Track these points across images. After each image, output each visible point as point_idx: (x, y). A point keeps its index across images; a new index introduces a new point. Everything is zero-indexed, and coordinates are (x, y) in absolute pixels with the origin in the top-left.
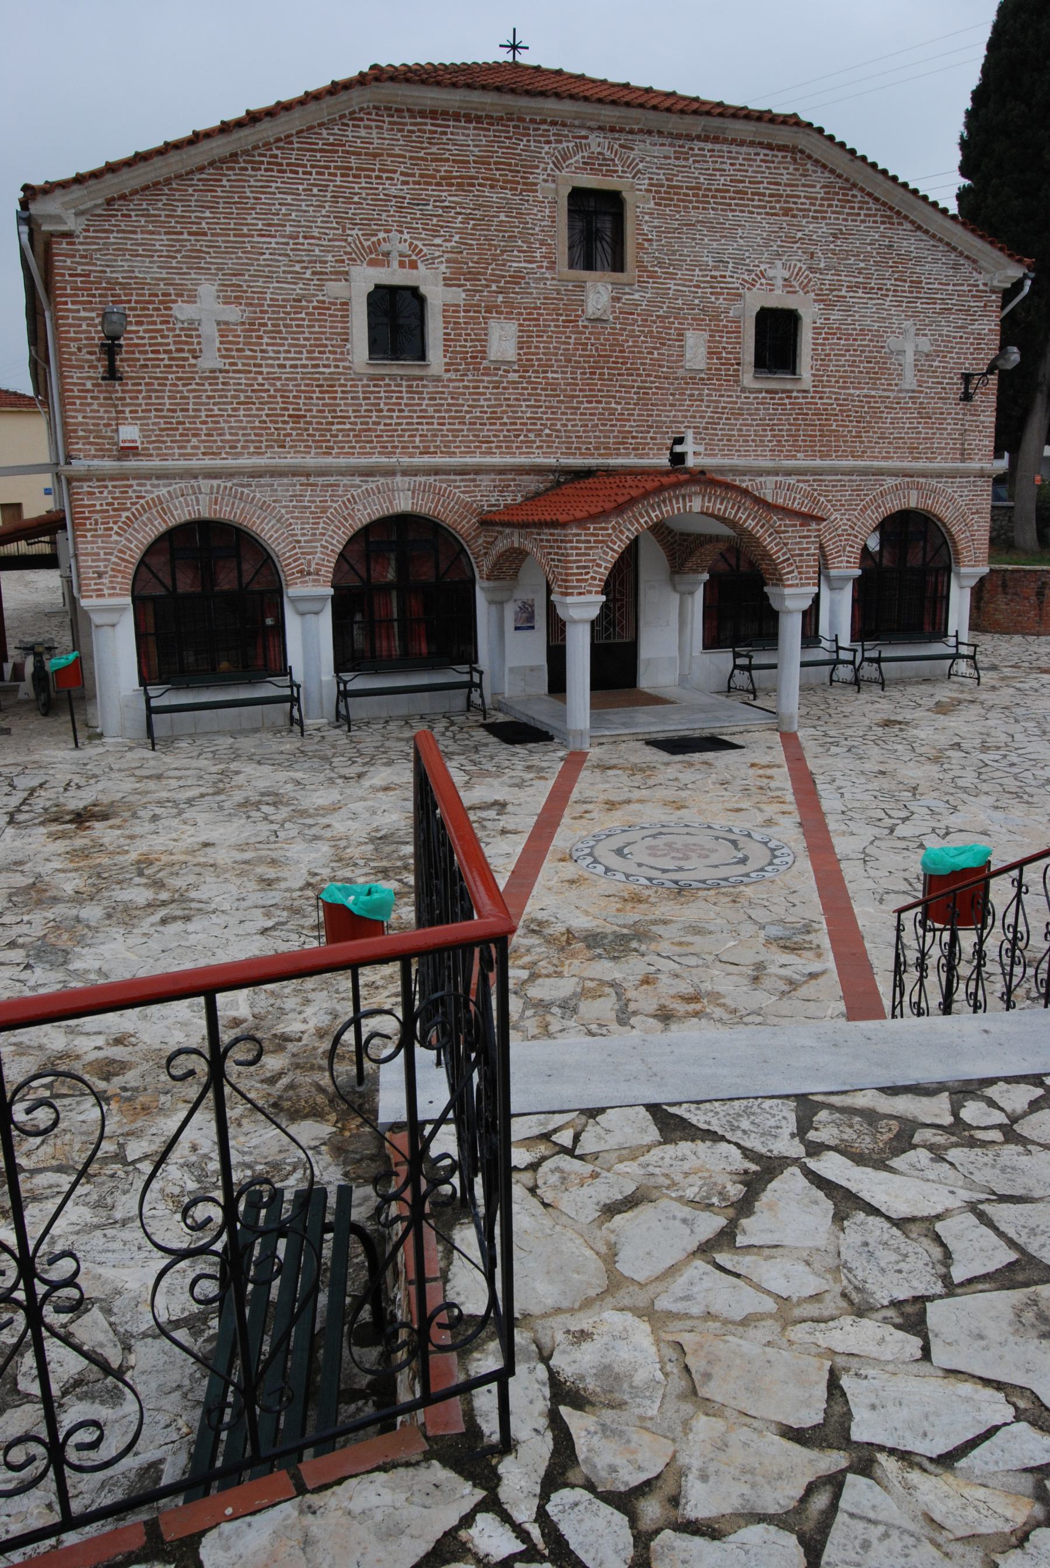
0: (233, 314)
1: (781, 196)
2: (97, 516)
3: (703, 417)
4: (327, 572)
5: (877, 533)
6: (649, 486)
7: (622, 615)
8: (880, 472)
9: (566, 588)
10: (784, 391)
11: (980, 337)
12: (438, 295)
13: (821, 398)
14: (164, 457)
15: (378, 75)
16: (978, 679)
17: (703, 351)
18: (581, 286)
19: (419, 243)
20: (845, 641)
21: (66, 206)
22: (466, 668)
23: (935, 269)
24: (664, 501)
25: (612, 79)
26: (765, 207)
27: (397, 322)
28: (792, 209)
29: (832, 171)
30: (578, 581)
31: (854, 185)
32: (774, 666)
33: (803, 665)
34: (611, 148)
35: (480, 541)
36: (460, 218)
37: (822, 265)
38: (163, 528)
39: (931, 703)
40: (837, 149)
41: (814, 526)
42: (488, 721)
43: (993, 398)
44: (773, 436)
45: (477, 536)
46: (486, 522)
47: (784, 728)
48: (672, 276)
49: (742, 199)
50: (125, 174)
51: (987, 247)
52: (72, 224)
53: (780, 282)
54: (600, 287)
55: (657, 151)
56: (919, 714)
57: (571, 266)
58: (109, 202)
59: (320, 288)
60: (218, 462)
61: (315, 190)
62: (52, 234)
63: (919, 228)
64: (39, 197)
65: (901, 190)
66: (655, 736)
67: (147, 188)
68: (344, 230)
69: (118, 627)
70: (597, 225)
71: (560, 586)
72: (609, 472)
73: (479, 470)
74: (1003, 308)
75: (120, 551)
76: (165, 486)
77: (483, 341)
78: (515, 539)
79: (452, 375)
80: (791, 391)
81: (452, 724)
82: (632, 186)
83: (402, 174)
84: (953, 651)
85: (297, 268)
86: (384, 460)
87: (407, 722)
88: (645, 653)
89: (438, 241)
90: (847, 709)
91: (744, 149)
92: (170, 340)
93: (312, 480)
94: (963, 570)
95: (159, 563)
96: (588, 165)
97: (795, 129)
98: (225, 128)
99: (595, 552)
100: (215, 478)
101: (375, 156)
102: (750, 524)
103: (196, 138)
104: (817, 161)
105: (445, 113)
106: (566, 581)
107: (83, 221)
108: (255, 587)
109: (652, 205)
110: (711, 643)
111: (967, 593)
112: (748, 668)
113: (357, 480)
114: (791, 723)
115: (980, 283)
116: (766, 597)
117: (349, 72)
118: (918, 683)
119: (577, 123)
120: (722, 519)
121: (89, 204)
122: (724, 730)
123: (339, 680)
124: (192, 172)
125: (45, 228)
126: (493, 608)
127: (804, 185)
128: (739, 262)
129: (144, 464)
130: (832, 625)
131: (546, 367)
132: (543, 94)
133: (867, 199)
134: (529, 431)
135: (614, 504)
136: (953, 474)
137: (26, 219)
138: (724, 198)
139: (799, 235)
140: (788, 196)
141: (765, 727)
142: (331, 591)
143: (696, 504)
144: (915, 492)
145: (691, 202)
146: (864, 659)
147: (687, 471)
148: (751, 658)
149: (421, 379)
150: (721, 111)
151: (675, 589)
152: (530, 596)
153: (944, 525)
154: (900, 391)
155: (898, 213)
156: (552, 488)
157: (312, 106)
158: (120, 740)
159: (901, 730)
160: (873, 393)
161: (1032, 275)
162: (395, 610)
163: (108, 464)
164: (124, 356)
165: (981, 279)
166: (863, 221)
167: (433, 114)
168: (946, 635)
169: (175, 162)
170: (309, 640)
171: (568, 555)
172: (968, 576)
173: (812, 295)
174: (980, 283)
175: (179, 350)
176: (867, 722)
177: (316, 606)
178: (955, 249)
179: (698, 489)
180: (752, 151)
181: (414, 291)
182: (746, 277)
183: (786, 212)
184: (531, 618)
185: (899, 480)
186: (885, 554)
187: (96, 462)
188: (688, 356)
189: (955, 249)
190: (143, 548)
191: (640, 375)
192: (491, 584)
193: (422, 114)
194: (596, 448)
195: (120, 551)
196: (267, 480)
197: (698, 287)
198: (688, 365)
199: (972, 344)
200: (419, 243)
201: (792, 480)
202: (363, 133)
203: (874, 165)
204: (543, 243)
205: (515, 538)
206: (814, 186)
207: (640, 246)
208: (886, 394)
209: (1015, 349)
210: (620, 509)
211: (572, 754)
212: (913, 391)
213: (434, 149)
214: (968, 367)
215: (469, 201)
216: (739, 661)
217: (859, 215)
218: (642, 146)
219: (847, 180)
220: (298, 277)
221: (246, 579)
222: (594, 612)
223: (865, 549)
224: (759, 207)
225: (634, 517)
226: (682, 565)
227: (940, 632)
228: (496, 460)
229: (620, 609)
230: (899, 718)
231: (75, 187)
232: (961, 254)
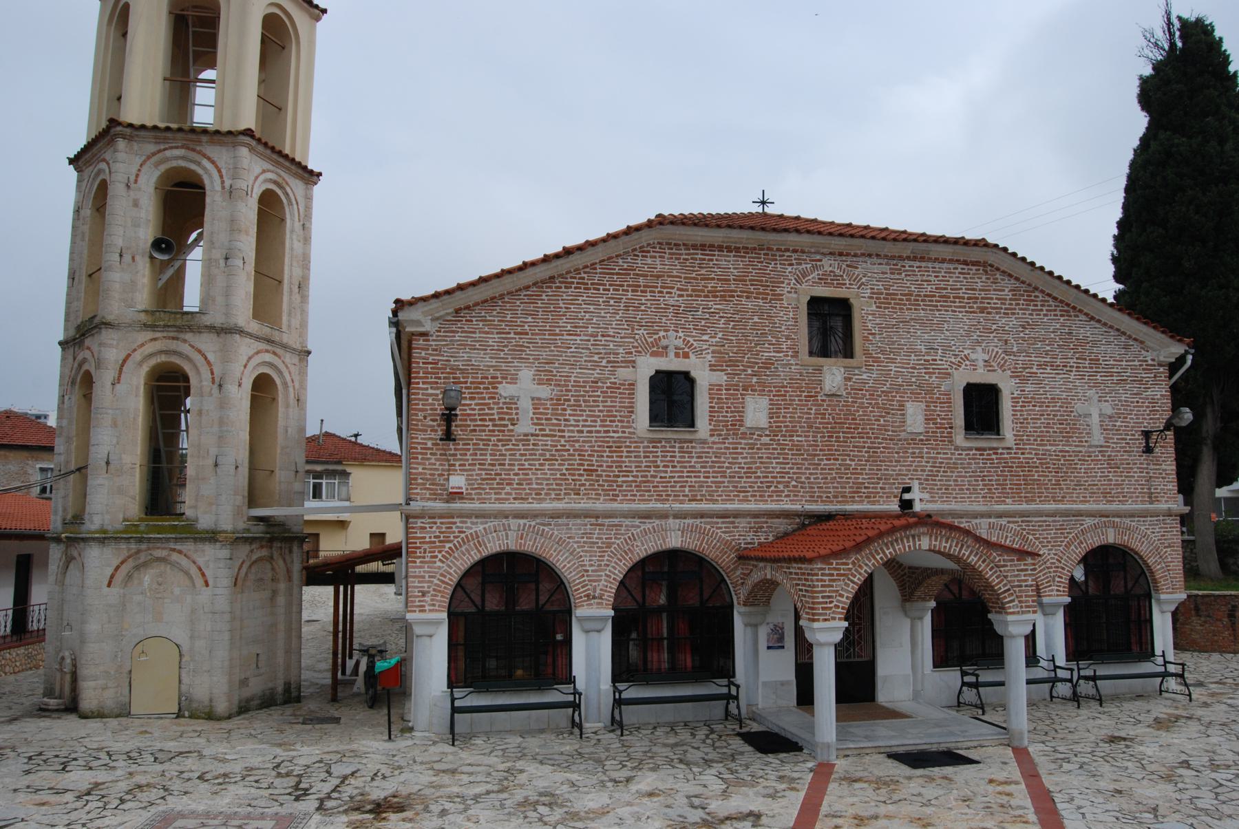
0: (544, 392)
2: (426, 546)
4: (609, 597)
6: (883, 527)
7: (860, 637)
8: (1079, 514)
9: (813, 614)
10: (990, 449)
11: (1153, 401)
12: (704, 378)
14: (483, 501)
15: (661, 221)
16: (1190, 695)
17: (920, 418)
18: (819, 369)
19: (691, 340)
20: (1061, 660)
21: (425, 314)
22: (724, 681)
23: (1108, 349)
24: (896, 541)
25: (837, 221)
27: (672, 398)
29: (1017, 279)
30: (823, 608)
31: (1036, 289)
32: (1002, 684)
33: (1029, 682)
34: (840, 267)
35: (738, 573)
36: (723, 321)
37: (1015, 349)
38: (477, 557)
39: (1150, 719)
40: (1020, 263)
41: (1029, 561)
42: (744, 730)
43: (1172, 450)
45: (735, 569)
46: (743, 557)
47: (1016, 744)
48: (893, 361)
50: (471, 291)
51: (1152, 331)
52: (428, 326)
53: (981, 364)
54: (835, 371)
55: (876, 268)
56: (1140, 730)
57: (811, 354)
58: (457, 311)
59: (613, 373)
60: (526, 506)
61: (612, 302)
62: (413, 334)
63: (1092, 318)
64: (406, 308)
65: (1075, 291)
66: (895, 749)
67: (486, 301)
68: (633, 329)
69: (434, 638)
70: (831, 324)
71: (807, 613)
72: (847, 516)
73: (737, 515)
74: (1170, 377)
75: (442, 575)
76: (482, 523)
77: (741, 412)
78: (768, 572)
79: (715, 439)
81: (712, 731)
82: (857, 295)
83: (679, 289)
84: (1162, 669)
85: (596, 358)
86: (659, 505)
87: (672, 728)
88: (882, 670)
89: (705, 337)
90: (1072, 725)
91: (945, 265)
92: (495, 411)
93: (600, 521)
94: (1163, 597)
95: (473, 585)
96: (822, 280)
97: (985, 249)
98: (546, 259)
99: (836, 585)
100: (523, 518)
101: (658, 277)
102: (973, 559)
103: (525, 266)
104: (1004, 272)
105: (712, 246)
106: (813, 609)
107: (437, 324)
108: (548, 607)
109: (874, 308)
110: (940, 661)
111: (1169, 617)
112: (976, 685)
113: (637, 521)
114: (1022, 739)
116: (990, 623)
117: (641, 219)
118: (1132, 699)
120: (949, 556)
121: (442, 313)
122: (959, 745)
123: (615, 689)
124: (520, 290)
125: (408, 329)
126: (749, 630)
129: (467, 506)
130: (1048, 646)
131: (792, 432)
132: (786, 230)
134: (779, 483)
135: (853, 543)
136: (1144, 514)
137: (395, 323)
139: (994, 327)
141: (997, 742)
142: (612, 613)
143: (925, 543)
146: (1080, 677)
147: (915, 515)
148: (977, 676)
149: (691, 441)
150: (924, 239)
151: (906, 614)
152: (780, 620)
153: (1141, 557)
154: (1090, 446)
155: (1074, 308)
156: (799, 529)
157: (612, 243)
158: (427, 734)
159: (1127, 747)
161: (1193, 351)
162: (665, 630)
163: (439, 506)
164: (459, 423)
168: (1154, 655)
169: (508, 284)
170: (591, 653)
171: (814, 586)
172: (1168, 602)
175: (500, 419)
176: (1093, 738)
177: (598, 626)
178: (1124, 333)
179: (925, 530)
181: (686, 375)
183: (982, 310)
184: (781, 638)
185: (1097, 520)
186: (1091, 583)
187: (430, 504)
188: (909, 422)
189: (1124, 333)
190: (460, 573)
192: (747, 609)
193: (694, 247)
194: (835, 497)
195: (442, 575)
196: (564, 520)
198: (909, 430)
200: (691, 340)
201: (1003, 521)
202: (649, 261)
203: (1051, 273)
204: (788, 338)
205: (769, 569)
207: (866, 339)
209: (1188, 410)
210: (858, 547)
211: (820, 765)
213: (703, 272)
214: (1147, 425)
215: (729, 308)
216: (967, 679)
218: (864, 265)
219: (1029, 285)
220: (596, 365)
221: (543, 599)
222: (838, 637)
223: (1072, 579)
225: (871, 553)
226: (912, 594)
227: (1147, 653)
228: (752, 506)
229: (859, 631)
230: (1123, 734)
231: (433, 301)
232: (1130, 337)
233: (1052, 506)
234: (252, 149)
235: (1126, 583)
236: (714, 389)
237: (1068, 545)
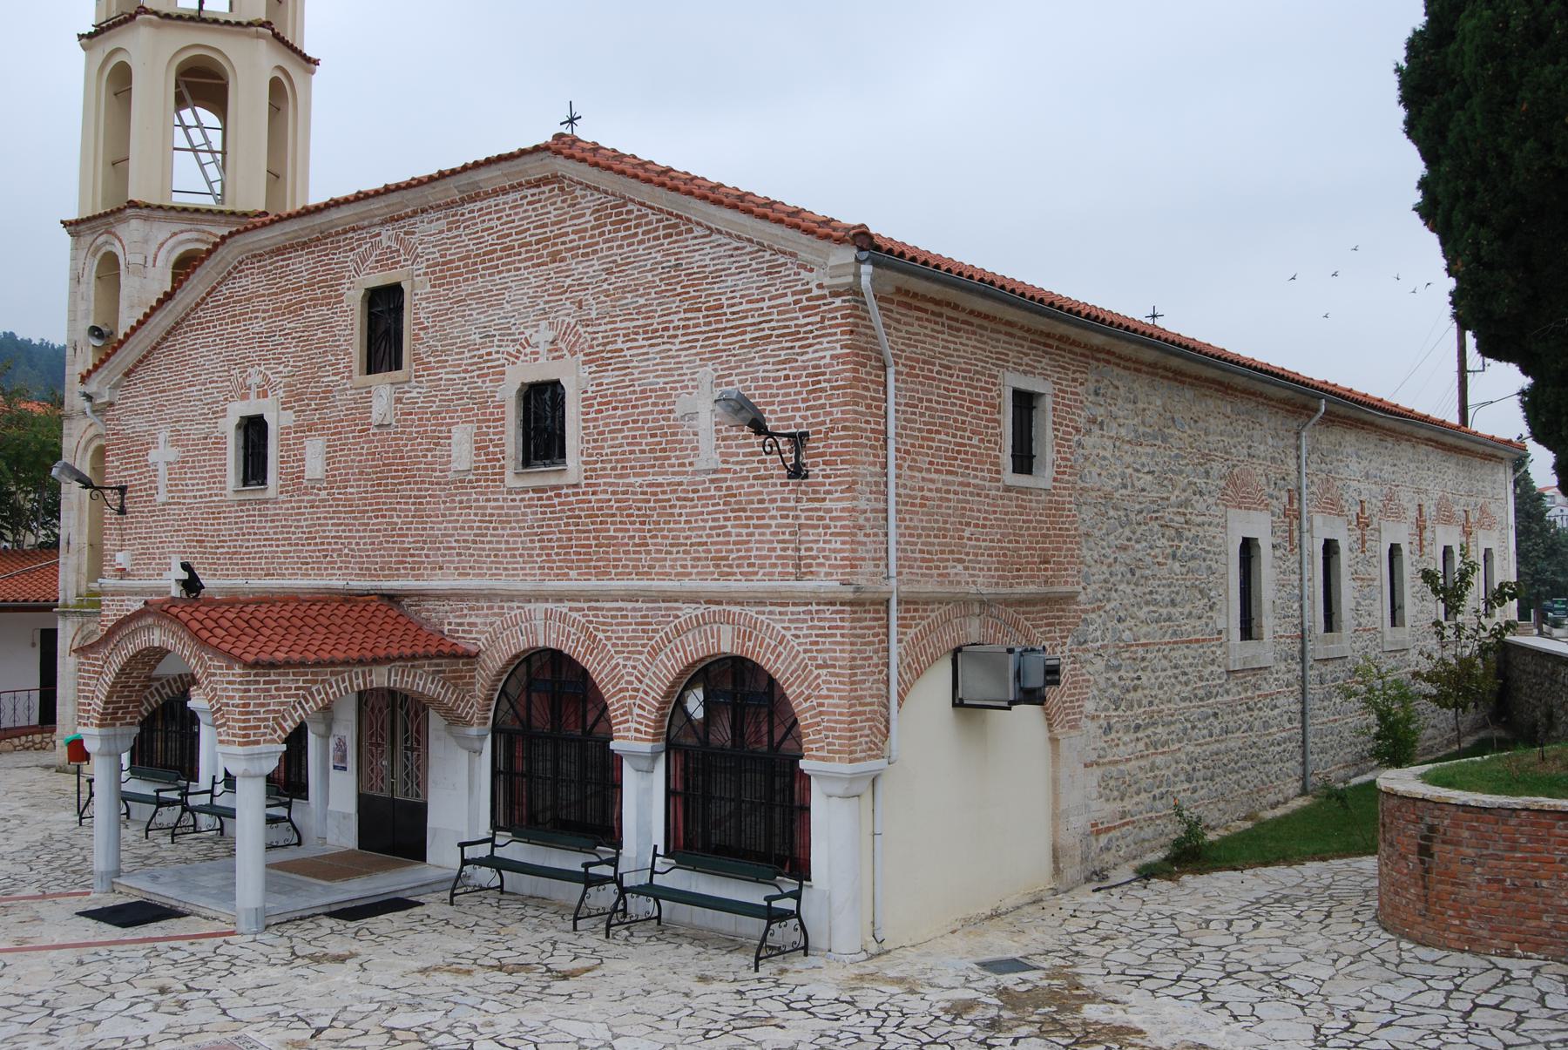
0: (173, 454)
1: (548, 239)
3: (471, 528)
5: (699, 693)
13: (594, 493)
26: (532, 258)
28: (560, 252)
29: (597, 189)
37: (593, 315)
44: (542, 548)
49: (508, 256)
58: (127, 375)
67: (140, 361)
79: (283, 497)
80: (561, 487)
83: (265, 311)
88: (431, 823)
89: (281, 368)
91: (512, 196)
105: (285, 248)
109: (428, 289)
115: (813, 285)
119: (366, 223)
127: (572, 218)
128: (505, 332)
133: (644, 210)
138: (491, 260)
139: (569, 281)
140: (556, 237)
144: (729, 628)
145: (461, 274)
149: (266, 502)
154: (695, 473)
160: (660, 479)
165: (813, 279)
166: (640, 243)
167: (278, 251)
173: (582, 358)
174: (813, 285)
180: (518, 195)
182: (510, 349)
184: (343, 758)
185: (702, 608)
189: (762, 247)
191: (416, 483)
194: (382, 569)
197: (466, 371)
198: (454, 466)
199: (805, 385)
201: (564, 607)
206: (583, 215)
208: (677, 479)
212: (715, 471)
217: (636, 234)
224: (525, 260)
233: (637, 584)
234: (146, 219)
235: (771, 732)
236: (285, 431)
237: (654, 653)
